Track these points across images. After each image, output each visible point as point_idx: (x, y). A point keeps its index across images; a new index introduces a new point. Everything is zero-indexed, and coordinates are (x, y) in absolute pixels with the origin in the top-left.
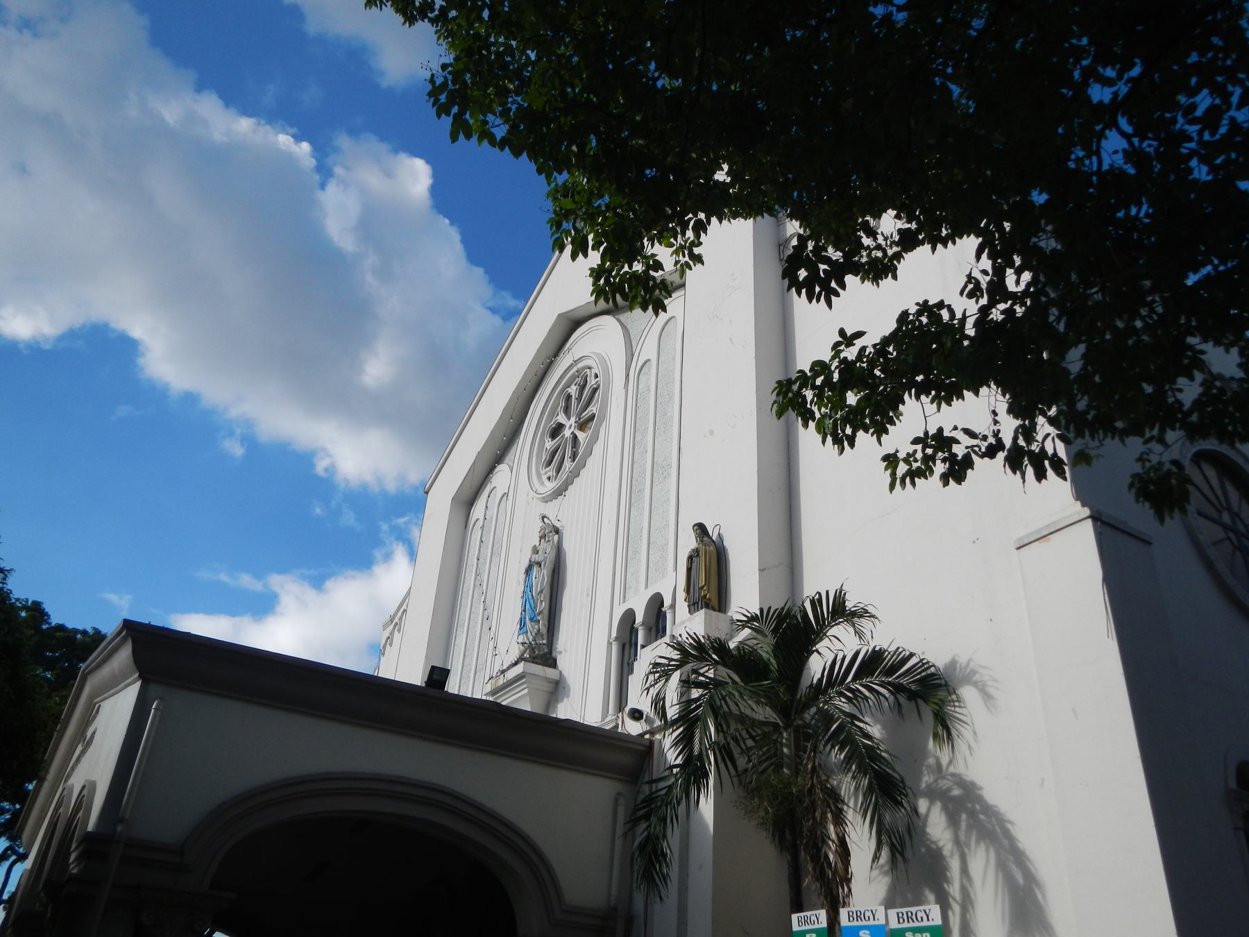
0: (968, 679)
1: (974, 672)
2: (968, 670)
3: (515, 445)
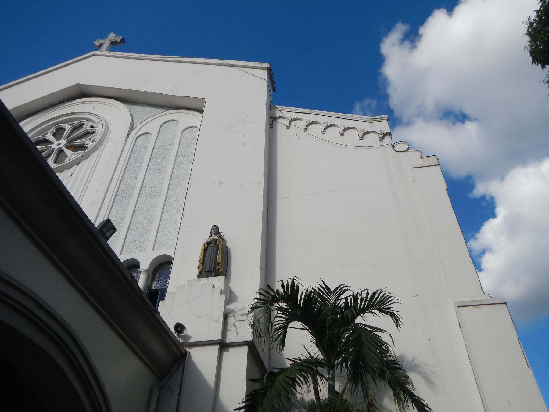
0: (415, 368)
1: (419, 366)
2: (413, 364)
3: (164, 110)
